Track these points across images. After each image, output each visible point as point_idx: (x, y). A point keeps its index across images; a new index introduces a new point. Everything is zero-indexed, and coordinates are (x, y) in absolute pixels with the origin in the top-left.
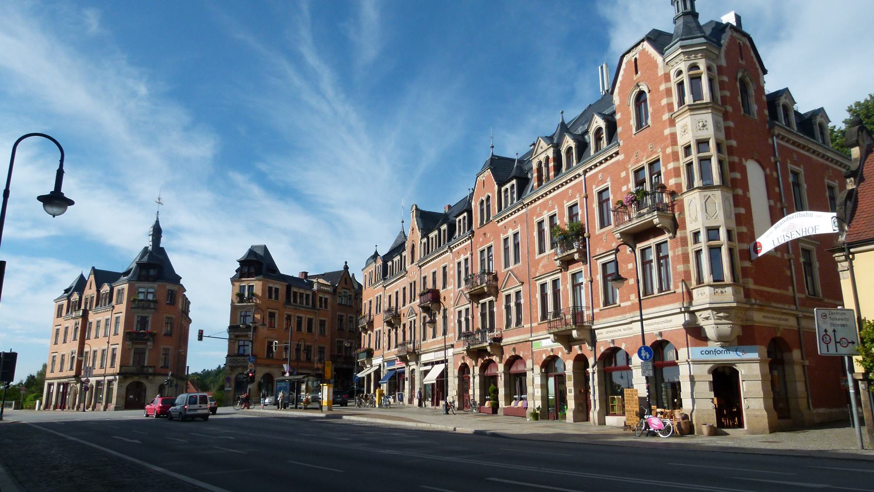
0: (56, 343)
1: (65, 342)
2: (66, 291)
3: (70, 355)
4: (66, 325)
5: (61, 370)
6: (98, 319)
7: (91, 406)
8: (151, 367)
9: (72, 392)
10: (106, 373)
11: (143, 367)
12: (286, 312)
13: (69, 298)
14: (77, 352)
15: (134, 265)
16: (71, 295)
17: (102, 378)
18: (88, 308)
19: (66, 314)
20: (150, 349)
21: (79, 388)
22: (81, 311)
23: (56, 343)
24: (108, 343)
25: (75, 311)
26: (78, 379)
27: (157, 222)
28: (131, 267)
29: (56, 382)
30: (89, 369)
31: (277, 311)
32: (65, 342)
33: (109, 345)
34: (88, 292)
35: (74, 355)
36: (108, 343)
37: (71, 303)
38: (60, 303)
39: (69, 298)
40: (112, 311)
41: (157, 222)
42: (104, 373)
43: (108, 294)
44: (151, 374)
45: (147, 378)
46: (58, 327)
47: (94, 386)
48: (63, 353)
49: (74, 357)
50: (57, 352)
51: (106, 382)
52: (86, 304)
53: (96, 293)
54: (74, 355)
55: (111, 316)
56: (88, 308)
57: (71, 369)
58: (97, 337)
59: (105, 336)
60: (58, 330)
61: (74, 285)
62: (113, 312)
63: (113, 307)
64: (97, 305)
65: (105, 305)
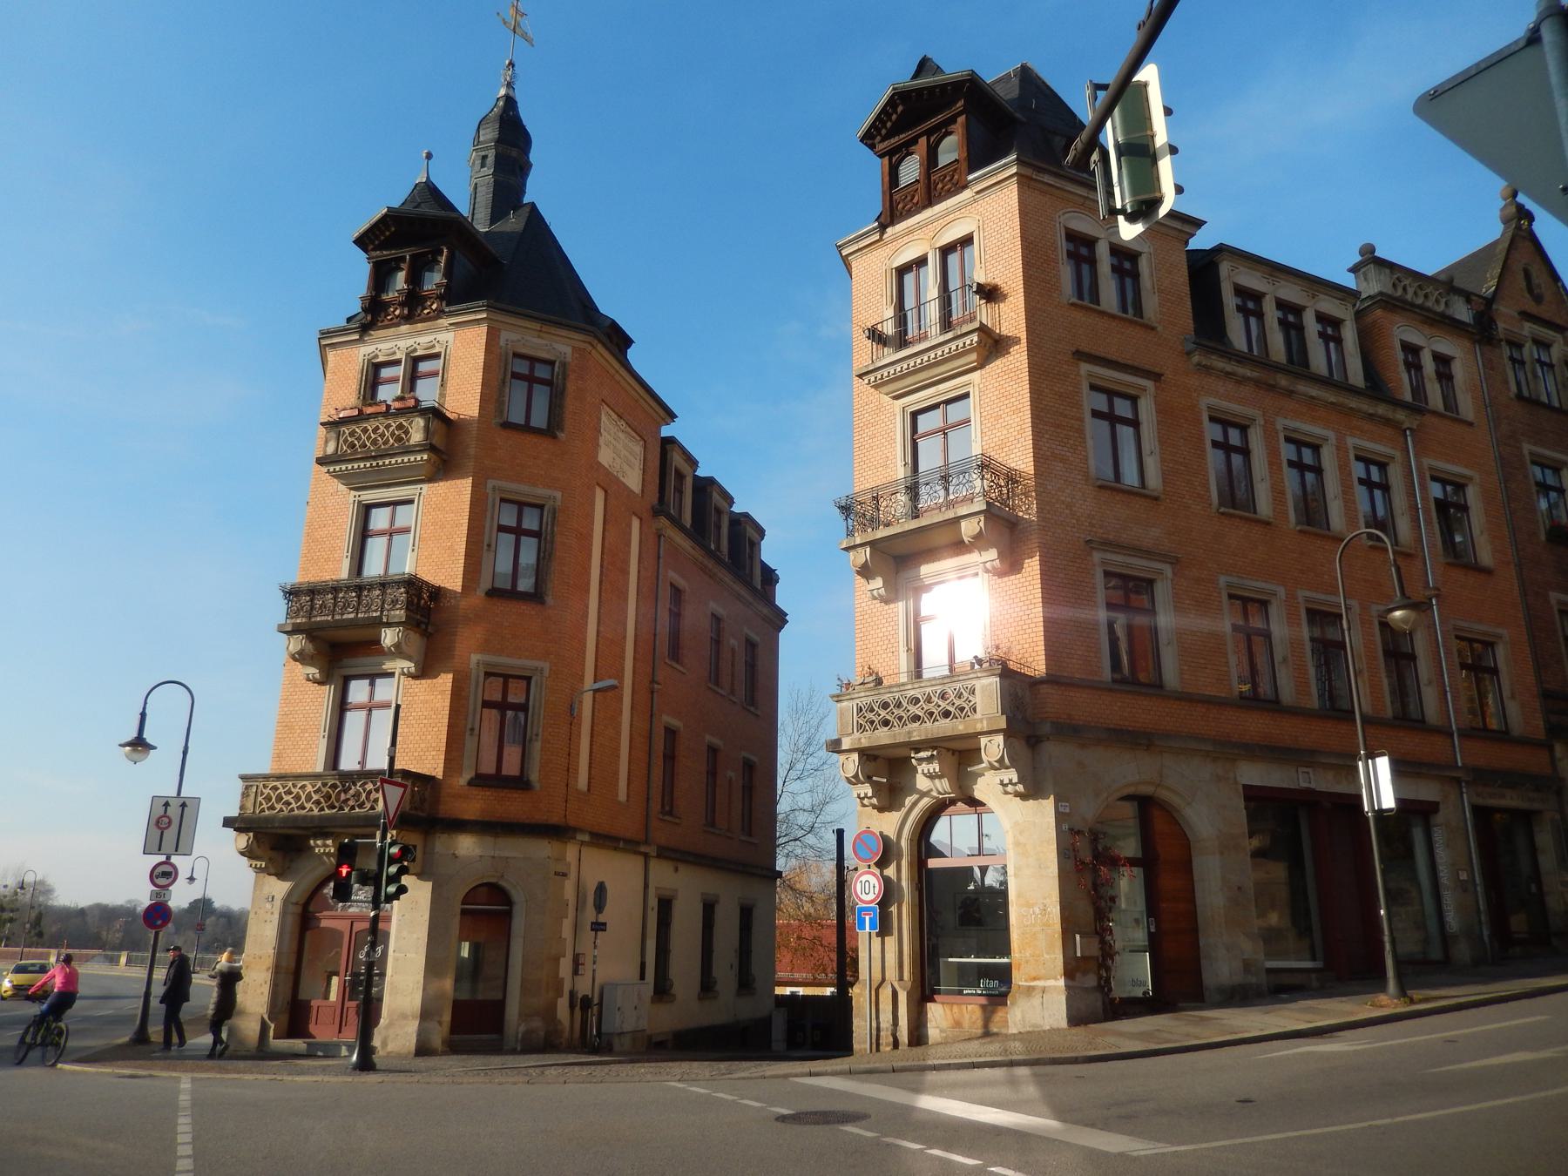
12: (1213, 401)
27: (510, 102)
30: (174, 812)
31: (1148, 384)
41: (510, 102)
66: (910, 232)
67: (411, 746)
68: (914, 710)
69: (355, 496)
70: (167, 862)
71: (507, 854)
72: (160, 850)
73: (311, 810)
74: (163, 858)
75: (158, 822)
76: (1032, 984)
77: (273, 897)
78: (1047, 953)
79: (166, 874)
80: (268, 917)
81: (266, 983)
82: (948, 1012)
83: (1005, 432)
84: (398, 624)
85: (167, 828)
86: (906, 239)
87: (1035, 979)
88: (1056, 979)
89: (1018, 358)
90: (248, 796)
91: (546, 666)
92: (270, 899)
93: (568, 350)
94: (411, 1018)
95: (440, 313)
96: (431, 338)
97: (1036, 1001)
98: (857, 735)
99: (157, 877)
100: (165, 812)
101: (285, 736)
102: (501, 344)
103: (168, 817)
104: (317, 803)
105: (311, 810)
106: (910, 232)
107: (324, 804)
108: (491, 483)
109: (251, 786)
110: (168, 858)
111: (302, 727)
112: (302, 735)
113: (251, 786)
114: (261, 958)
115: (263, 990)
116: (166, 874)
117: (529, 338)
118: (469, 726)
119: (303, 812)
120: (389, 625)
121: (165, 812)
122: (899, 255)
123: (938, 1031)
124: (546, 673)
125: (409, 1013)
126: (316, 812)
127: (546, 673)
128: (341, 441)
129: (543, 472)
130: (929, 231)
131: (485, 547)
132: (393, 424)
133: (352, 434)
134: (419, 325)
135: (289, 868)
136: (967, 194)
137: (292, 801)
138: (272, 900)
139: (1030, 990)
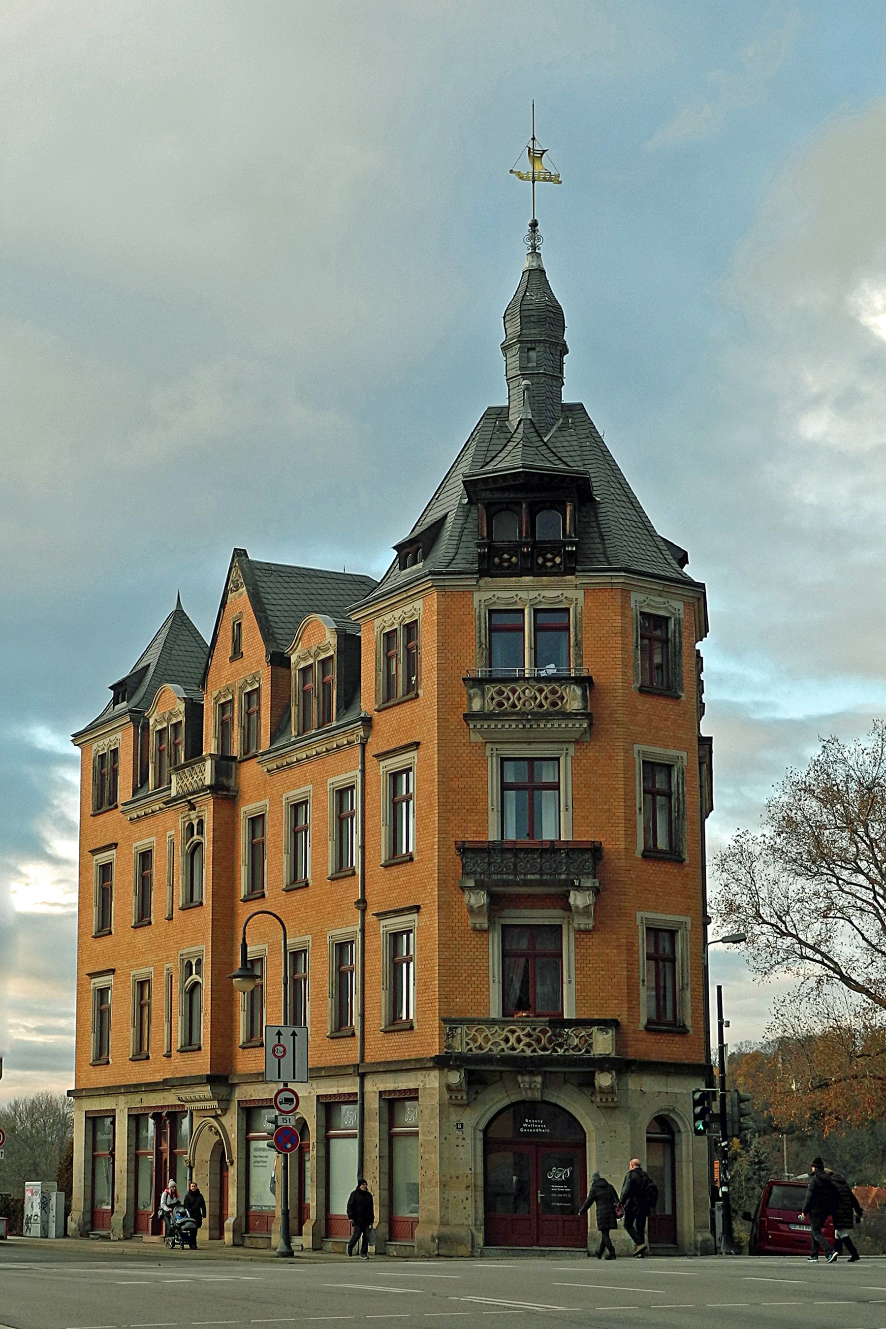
0: (104, 928)
1: (143, 918)
2: (122, 690)
3: (177, 977)
4: (142, 844)
5: (140, 1055)
6: (295, 794)
7: (307, 1228)
8: (604, 1024)
9: (204, 1154)
10: (368, 1060)
11: (558, 1023)
13: (139, 719)
14: (207, 961)
15: (456, 496)
16: (149, 700)
17: (350, 1086)
18: (236, 750)
19: (135, 791)
20: (579, 931)
21: (233, 1136)
22: (209, 764)
23: (104, 928)
24: (362, 904)
25: (178, 769)
26: (223, 1091)
28: (435, 515)
29: (121, 1107)
32: (143, 918)
33: (370, 918)
34: (225, 673)
35: (194, 977)
36: (362, 904)
37: (153, 738)
38: (102, 745)
39: (139, 719)
40: (363, 745)
42: (354, 1057)
43: (334, 666)
44: (603, 1064)
45: (587, 1083)
46: (103, 858)
47: (312, 1126)
48: (141, 972)
49: (196, 984)
50: (113, 971)
51: (373, 1104)
52: (224, 727)
53: (265, 672)
54: (194, 977)
55: (363, 771)
56: (236, 750)
57: (190, 1045)
58: (297, 883)
59: (342, 871)
60: (106, 870)
61: (152, 659)
62: (371, 751)
63: (367, 722)
64: (279, 729)
65: (326, 718)
67: (590, 994)
69: (492, 750)
70: (286, 1089)
71: (675, 1090)
72: (294, 1078)
73: (523, 1051)
74: (281, 1086)
75: (274, 1051)
77: (462, 1124)
79: (288, 1101)
84: (588, 889)
85: (283, 1056)
91: (688, 920)
93: (680, 605)
96: (558, 593)
99: (281, 1103)
100: (279, 1041)
101: (451, 978)
102: (633, 606)
103: (282, 1046)
105: (523, 1051)
107: (535, 1046)
108: (637, 747)
110: (286, 1085)
116: (288, 1101)
117: (653, 598)
118: (641, 978)
119: (515, 1053)
120: (579, 888)
121: (279, 1041)
124: (689, 926)
126: (528, 1052)
127: (689, 926)
129: (671, 734)
131: (638, 811)
132: (545, 688)
133: (500, 693)
135: (475, 1099)
137: (510, 1044)
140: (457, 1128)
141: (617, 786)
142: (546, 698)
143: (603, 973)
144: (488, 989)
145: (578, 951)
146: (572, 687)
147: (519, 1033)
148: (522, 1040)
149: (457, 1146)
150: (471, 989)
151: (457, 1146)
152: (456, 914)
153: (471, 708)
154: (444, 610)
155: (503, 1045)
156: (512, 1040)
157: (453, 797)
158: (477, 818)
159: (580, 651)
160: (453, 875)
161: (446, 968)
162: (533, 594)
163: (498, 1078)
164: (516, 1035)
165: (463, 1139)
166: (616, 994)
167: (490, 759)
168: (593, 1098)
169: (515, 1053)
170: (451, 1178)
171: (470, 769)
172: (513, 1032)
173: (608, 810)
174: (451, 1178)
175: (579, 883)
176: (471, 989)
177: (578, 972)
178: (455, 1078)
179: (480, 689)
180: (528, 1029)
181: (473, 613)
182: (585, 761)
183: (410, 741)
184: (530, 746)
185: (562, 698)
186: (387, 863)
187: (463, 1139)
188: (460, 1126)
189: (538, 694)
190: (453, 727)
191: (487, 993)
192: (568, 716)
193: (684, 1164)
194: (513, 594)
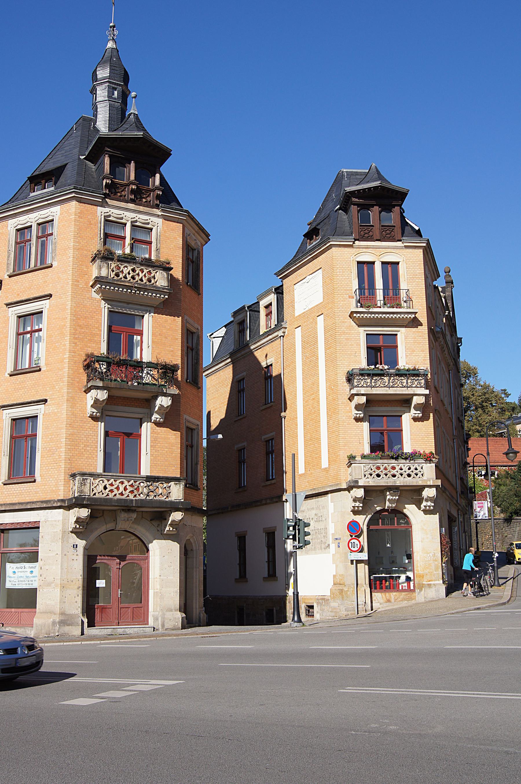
66: (367, 247)
68: (394, 472)
76: (429, 583)
78: (435, 571)
80: (75, 557)
81: (78, 596)
82: (384, 596)
83: (417, 358)
86: (364, 250)
87: (430, 581)
88: (439, 580)
89: (424, 329)
90: (85, 485)
92: (75, 546)
94: (174, 611)
95: (157, 207)
97: (433, 589)
98: (364, 479)
104: (132, 492)
106: (367, 247)
109: (87, 479)
111: (85, 444)
112: (85, 448)
113: (87, 479)
114: (72, 581)
115: (76, 599)
120: (165, 395)
122: (359, 256)
123: (379, 604)
125: (173, 608)
128: (110, 270)
130: (378, 252)
134: (141, 207)
136: (399, 244)
138: (77, 547)
139: (429, 585)
140: (74, 547)
141: (177, 337)
142: (145, 276)
143: (167, 450)
144: (97, 456)
145: (153, 435)
146: (161, 271)
147: (126, 483)
148: (127, 489)
149: (73, 560)
150: (86, 455)
151: (73, 560)
152: (78, 405)
153: (101, 274)
154: (79, 213)
155: (116, 491)
156: (122, 489)
157: (80, 330)
158: (94, 345)
159: (159, 254)
160: (78, 380)
161: (71, 440)
162: (133, 215)
163: (101, 515)
164: (124, 485)
165: (77, 555)
166: (174, 463)
167: (103, 309)
168: (159, 529)
169: (123, 497)
170: (68, 582)
171: (91, 314)
172: (122, 483)
173: (172, 351)
174: (68, 582)
175: (166, 391)
176: (86, 455)
177: (152, 448)
178: (84, 513)
179: (106, 263)
180: (132, 481)
181: (96, 218)
182: (160, 320)
183: (47, 293)
184: (128, 306)
185: (154, 277)
186: (12, 373)
187: (77, 555)
188: (75, 546)
189: (140, 273)
190: (82, 286)
191: (95, 458)
192: (158, 290)
193: (194, 569)
194: (122, 212)
